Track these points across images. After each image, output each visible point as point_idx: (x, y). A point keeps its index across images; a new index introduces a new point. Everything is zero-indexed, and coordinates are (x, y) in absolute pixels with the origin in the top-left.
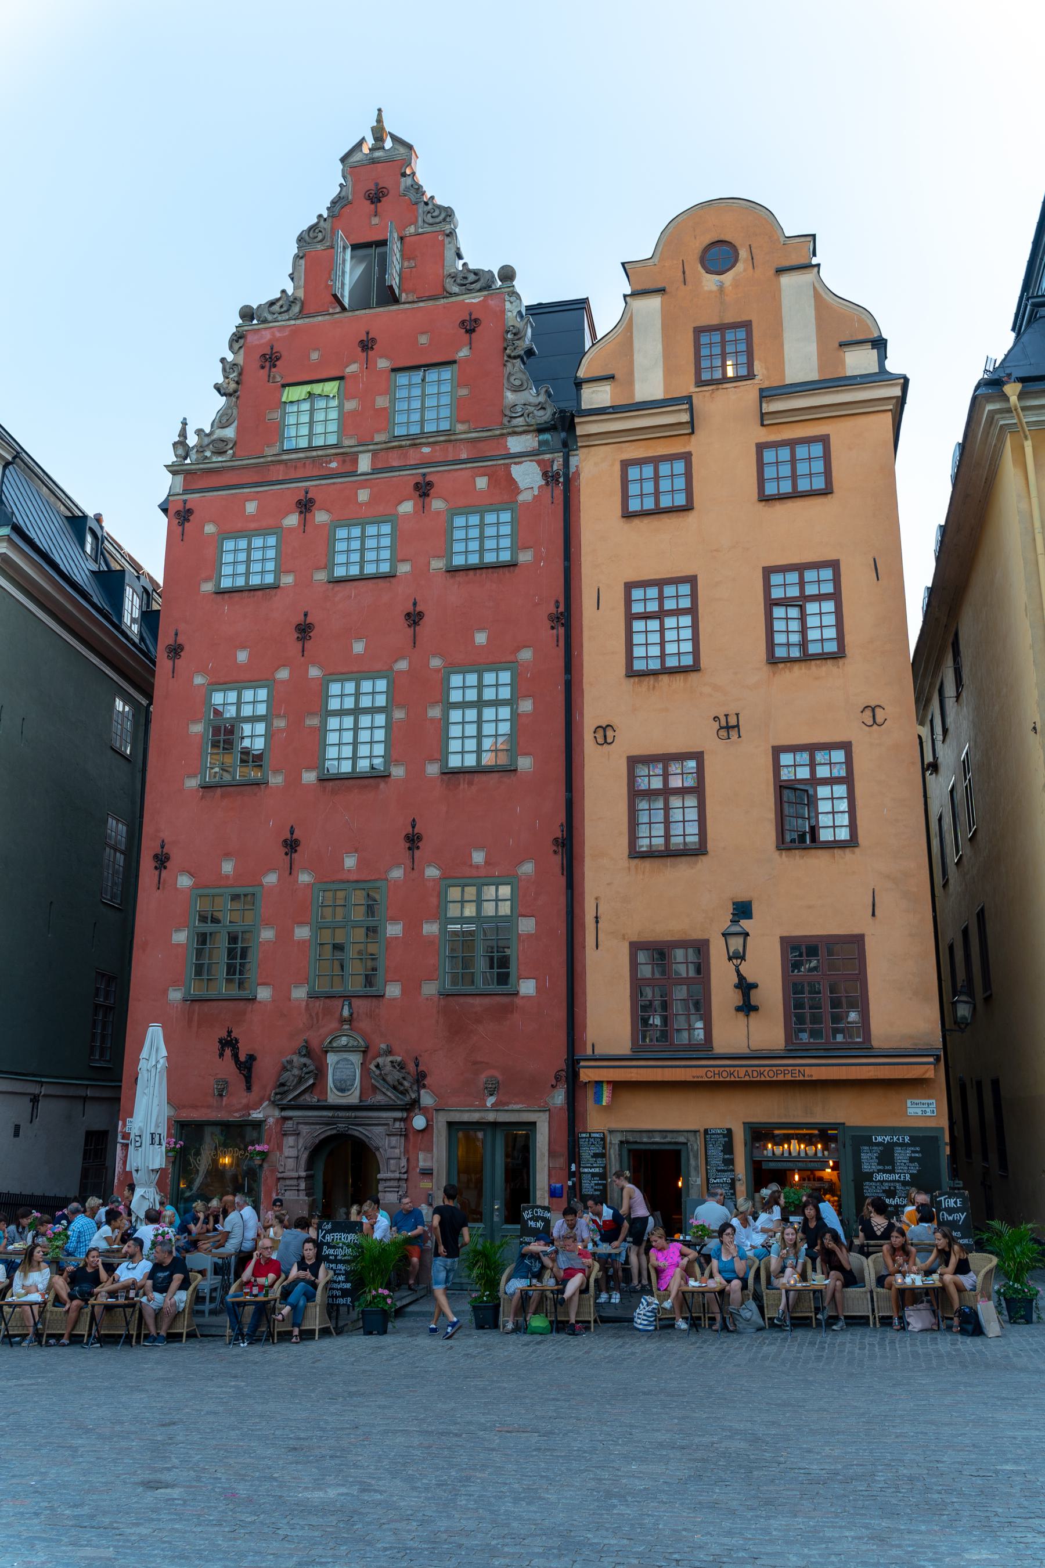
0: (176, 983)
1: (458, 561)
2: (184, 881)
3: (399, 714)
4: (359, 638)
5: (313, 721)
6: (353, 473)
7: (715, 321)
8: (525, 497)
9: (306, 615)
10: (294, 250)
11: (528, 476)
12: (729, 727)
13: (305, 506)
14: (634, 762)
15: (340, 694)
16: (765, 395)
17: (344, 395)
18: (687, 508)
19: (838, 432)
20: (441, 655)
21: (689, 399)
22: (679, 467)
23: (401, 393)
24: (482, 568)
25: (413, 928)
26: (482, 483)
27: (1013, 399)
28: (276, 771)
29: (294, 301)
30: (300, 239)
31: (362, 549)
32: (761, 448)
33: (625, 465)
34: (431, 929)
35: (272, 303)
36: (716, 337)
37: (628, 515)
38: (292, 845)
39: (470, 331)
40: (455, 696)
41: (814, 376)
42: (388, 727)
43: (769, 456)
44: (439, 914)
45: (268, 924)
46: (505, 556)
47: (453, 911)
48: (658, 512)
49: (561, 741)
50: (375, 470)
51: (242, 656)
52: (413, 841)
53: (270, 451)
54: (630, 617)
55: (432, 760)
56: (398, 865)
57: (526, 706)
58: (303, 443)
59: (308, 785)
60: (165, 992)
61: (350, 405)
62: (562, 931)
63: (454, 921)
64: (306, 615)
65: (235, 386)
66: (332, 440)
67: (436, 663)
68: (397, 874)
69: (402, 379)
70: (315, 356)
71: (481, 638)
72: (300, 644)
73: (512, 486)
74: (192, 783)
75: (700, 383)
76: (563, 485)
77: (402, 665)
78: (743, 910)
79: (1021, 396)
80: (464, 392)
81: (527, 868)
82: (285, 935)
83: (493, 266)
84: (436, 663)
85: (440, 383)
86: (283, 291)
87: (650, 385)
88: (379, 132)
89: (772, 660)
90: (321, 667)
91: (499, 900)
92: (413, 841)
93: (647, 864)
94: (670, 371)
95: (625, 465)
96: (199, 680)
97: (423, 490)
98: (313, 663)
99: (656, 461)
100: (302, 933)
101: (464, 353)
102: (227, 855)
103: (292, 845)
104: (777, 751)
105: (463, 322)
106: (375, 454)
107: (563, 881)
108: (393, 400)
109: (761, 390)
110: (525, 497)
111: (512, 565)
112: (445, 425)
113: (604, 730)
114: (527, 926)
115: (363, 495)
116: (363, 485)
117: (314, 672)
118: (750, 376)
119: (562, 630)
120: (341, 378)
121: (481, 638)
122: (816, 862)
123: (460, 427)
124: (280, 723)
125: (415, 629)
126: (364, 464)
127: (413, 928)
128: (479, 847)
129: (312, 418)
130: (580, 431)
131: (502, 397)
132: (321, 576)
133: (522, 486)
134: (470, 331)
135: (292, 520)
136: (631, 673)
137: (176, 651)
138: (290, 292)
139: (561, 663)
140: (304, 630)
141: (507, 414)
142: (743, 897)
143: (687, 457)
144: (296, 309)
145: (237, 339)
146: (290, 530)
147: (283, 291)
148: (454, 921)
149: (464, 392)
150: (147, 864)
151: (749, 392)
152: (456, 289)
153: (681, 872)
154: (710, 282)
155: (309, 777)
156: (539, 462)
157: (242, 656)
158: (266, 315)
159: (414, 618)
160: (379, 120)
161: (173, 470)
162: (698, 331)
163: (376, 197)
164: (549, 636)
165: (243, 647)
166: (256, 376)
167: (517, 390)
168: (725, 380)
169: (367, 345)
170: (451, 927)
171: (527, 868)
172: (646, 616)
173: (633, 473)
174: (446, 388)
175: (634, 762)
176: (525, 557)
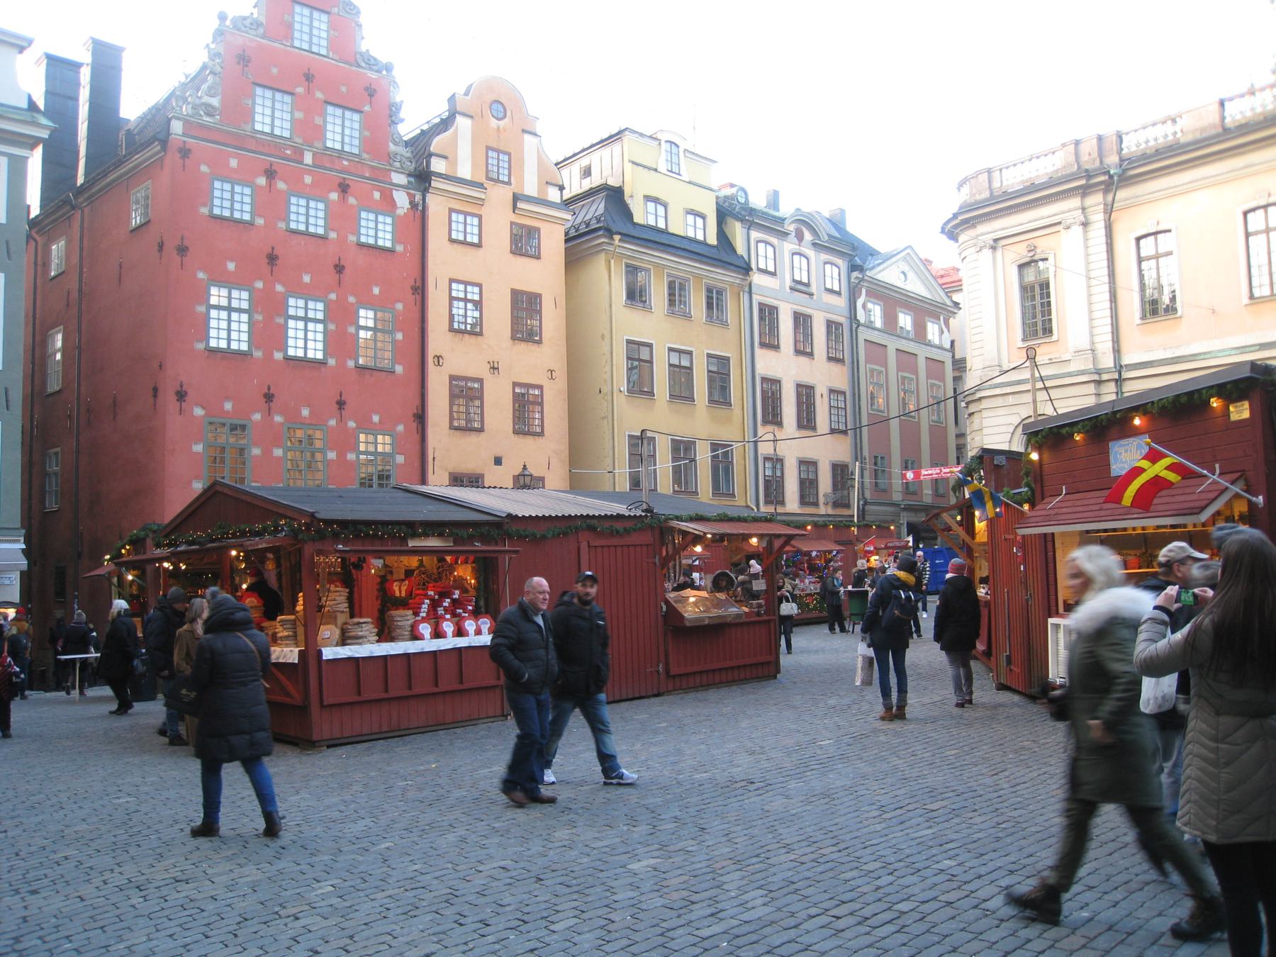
0: (198, 477)
1: (363, 239)
2: (199, 412)
3: (332, 327)
4: (307, 272)
5: (281, 321)
6: (301, 162)
7: (495, 146)
8: (400, 212)
11: (402, 199)
12: (494, 368)
13: (270, 174)
14: (452, 378)
15: (295, 305)
16: (516, 198)
18: (478, 246)
19: (545, 228)
20: (356, 296)
21: (481, 186)
22: (476, 221)
23: (330, 119)
24: (375, 247)
25: (342, 455)
26: (377, 195)
27: (617, 242)
28: (258, 348)
29: (259, 25)
31: (308, 215)
32: (512, 223)
33: (451, 211)
34: (351, 456)
35: (245, 18)
38: (269, 397)
39: (371, 96)
41: (535, 195)
42: (325, 332)
44: (355, 448)
45: (256, 444)
47: (362, 447)
48: (464, 243)
49: (417, 360)
52: (341, 404)
53: (248, 128)
54: (452, 299)
55: (350, 358)
56: (332, 417)
57: (399, 336)
59: (277, 362)
60: (190, 482)
61: (299, 115)
62: (417, 464)
63: (363, 453)
66: (287, 134)
67: (352, 299)
68: (332, 422)
69: (330, 109)
71: (376, 291)
72: (269, 268)
73: (393, 204)
75: (488, 178)
76: (420, 214)
77: (333, 296)
78: (498, 461)
80: (367, 134)
81: (400, 428)
82: (267, 452)
83: (383, 58)
84: (352, 299)
87: (465, 171)
89: (514, 338)
90: (284, 285)
91: (384, 443)
92: (341, 404)
93: (458, 433)
94: (474, 166)
95: (451, 211)
96: (201, 275)
97: (344, 188)
98: (280, 282)
99: (466, 214)
100: (278, 452)
101: (367, 108)
102: (227, 398)
103: (269, 397)
104: (515, 384)
105: (366, 89)
107: (417, 437)
108: (325, 122)
109: (514, 194)
110: (400, 212)
111: (390, 251)
112: (356, 151)
114: (400, 459)
115: (308, 179)
116: (309, 172)
117: (279, 288)
118: (509, 183)
119: (418, 298)
120: (292, 94)
121: (376, 291)
122: (529, 440)
123: (365, 156)
124: (259, 317)
125: (340, 274)
126: (308, 158)
127: (342, 455)
128: (376, 413)
130: (433, 184)
131: (388, 146)
132: (282, 225)
133: (399, 204)
134: (371, 96)
135: (262, 181)
136: (451, 329)
137: (182, 250)
138: (255, 16)
139: (417, 315)
140: (272, 258)
141: (390, 157)
142: (498, 455)
143: (480, 217)
144: (261, 31)
145: (219, 33)
146: (260, 187)
148: (363, 453)
149: (367, 134)
150: (168, 398)
152: (363, 64)
153: (473, 439)
154: (494, 123)
155: (278, 356)
156: (409, 194)
158: (240, 25)
162: (488, 148)
164: (410, 298)
165: (232, 260)
168: (498, 181)
170: (362, 457)
171: (400, 428)
172: (458, 299)
173: (454, 216)
174: (356, 126)
175: (452, 378)
176: (399, 248)
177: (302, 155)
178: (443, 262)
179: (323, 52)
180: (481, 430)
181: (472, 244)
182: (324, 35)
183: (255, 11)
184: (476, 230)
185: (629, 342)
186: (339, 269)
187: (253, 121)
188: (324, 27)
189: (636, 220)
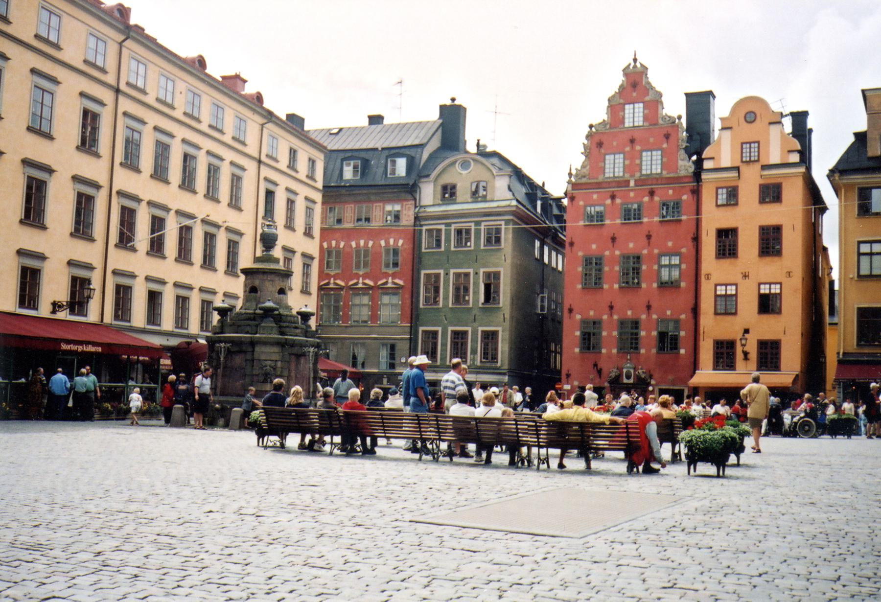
6: (628, 185)
13: (613, 197)
17: (624, 159)
21: (737, 169)
23: (644, 159)
26: (671, 192)
36: (748, 145)
37: (717, 206)
40: (663, 263)
50: (636, 185)
51: (594, 246)
58: (612, 175)
65: (588, 152)
66: (621, 174)
67: (656, 251)
69: (644, 154)
70: (615, 143)
74: (579, 286)
85: (657, 154)
90: (619, 250)
95: (717, 189)
97: (652, 193)
101: (665, 146)
106: (636, 181)
116: (632, 190)
123: (664, 172)
126: (632, 183)
129: (614, 166)
135: (609, 201)
137: (572, 244)
140: (613, 239)
151: (758, 166)
157: (594, 246)
159: (649, 237)
161: (569, 182)
165: (594, 243)
166: (595, 151)
167: (682, 160)
169: (632, 141)
174: (660, 157)
177: (628, 181)
178: (714, 218)
179: (641, 124)
180: (735, 314)
182: (641, 114)
185: (859, 243)
187: (604, 173)
188: (641, 110)
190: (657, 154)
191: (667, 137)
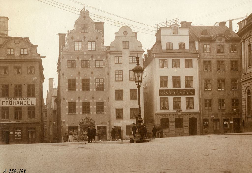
9: (79, 71)
10: (74, 23)
30: (75, 22)
43: (130, 57)
46: (102, 67)
52: (93, 98)
64: (79, 71)
75: (123, 49)
79: (155, 55)
86: (73, 29)
88: (84, 8)
97: (92, 57)
113: (113, 87)
138: (74, 29)
147: (73, 29)
160: (84, 7)
163: (85, 17)
178: (114, 67)
181: (120, 63)
183: (74, 28)
184: (121, 60)
186: (92, 73)
189: (162, 49)
190: (94, 44)
191: (97, 38)
